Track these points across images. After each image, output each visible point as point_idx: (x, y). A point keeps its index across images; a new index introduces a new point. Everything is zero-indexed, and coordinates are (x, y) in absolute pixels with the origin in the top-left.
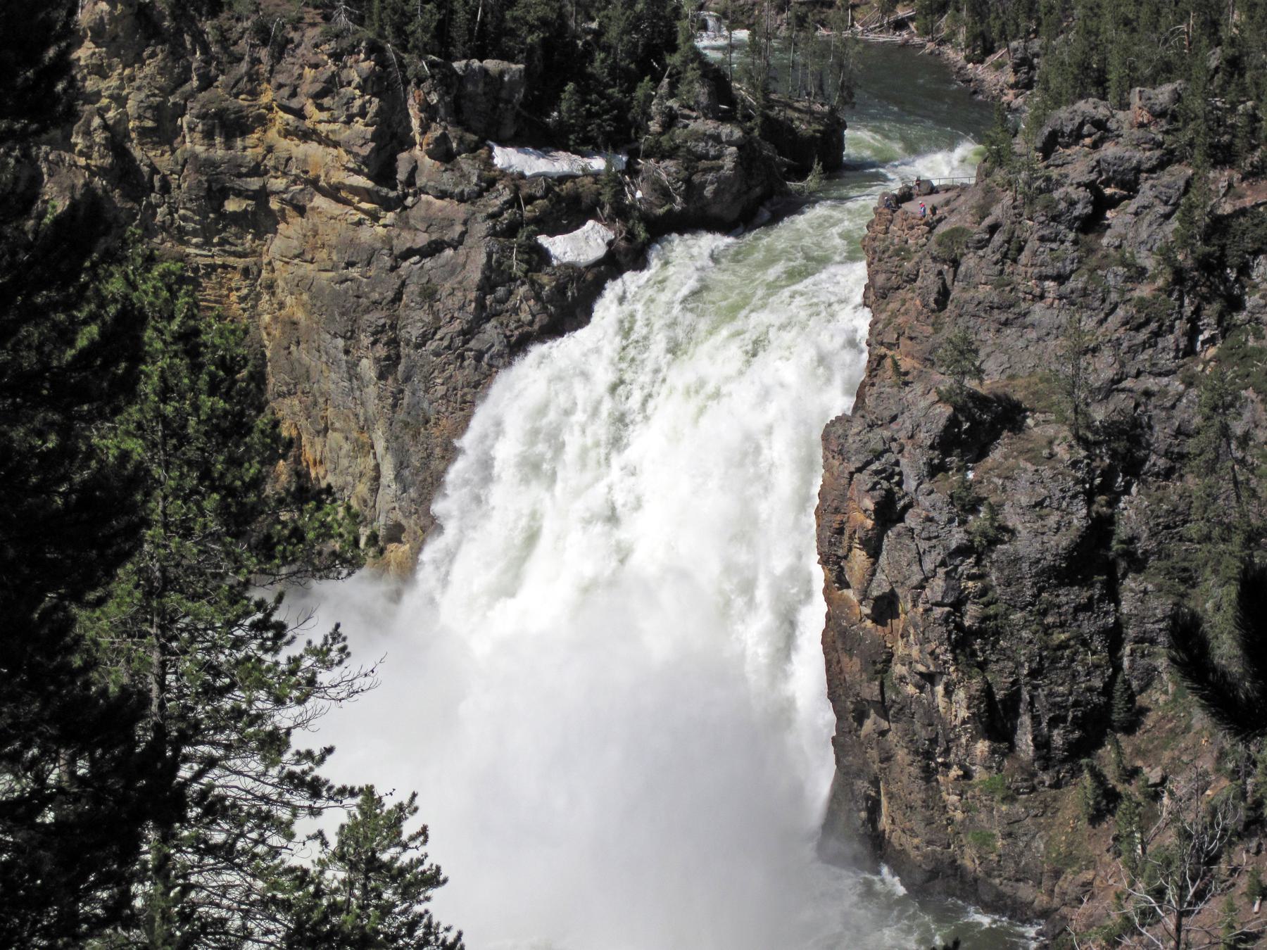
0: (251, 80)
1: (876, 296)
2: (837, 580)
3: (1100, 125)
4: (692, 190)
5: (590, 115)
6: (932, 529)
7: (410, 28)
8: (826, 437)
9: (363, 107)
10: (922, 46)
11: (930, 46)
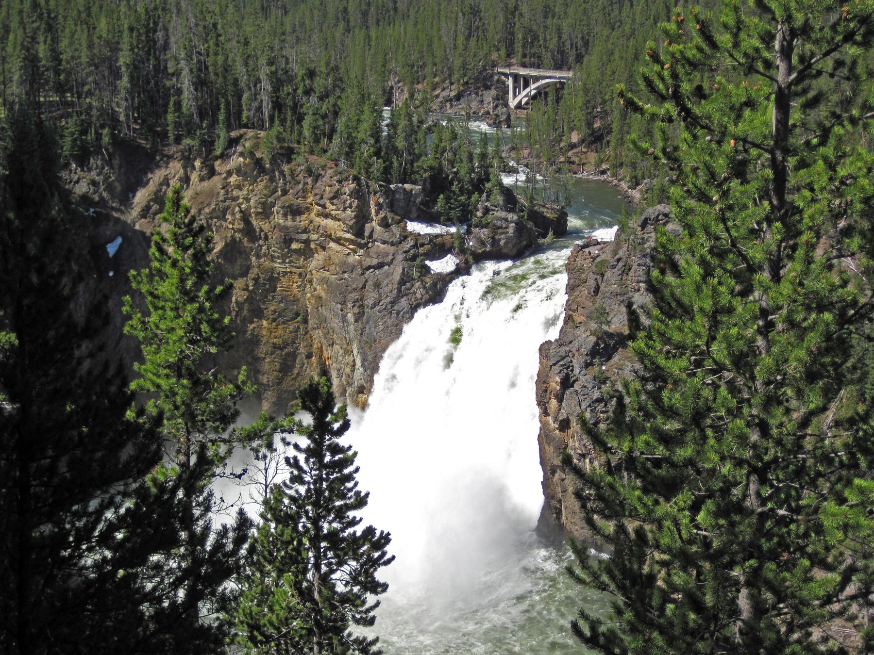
0: (304, 192)
1: (571, 289)
2: (545, 412)
3: (666, 215)
4: (495, 242)
5: (450, 208)
6: (586, 390)
7: (371, 170)
8: (540, 350)
9: (351, 204)
10: (612, 182)
11: (615, 182)
